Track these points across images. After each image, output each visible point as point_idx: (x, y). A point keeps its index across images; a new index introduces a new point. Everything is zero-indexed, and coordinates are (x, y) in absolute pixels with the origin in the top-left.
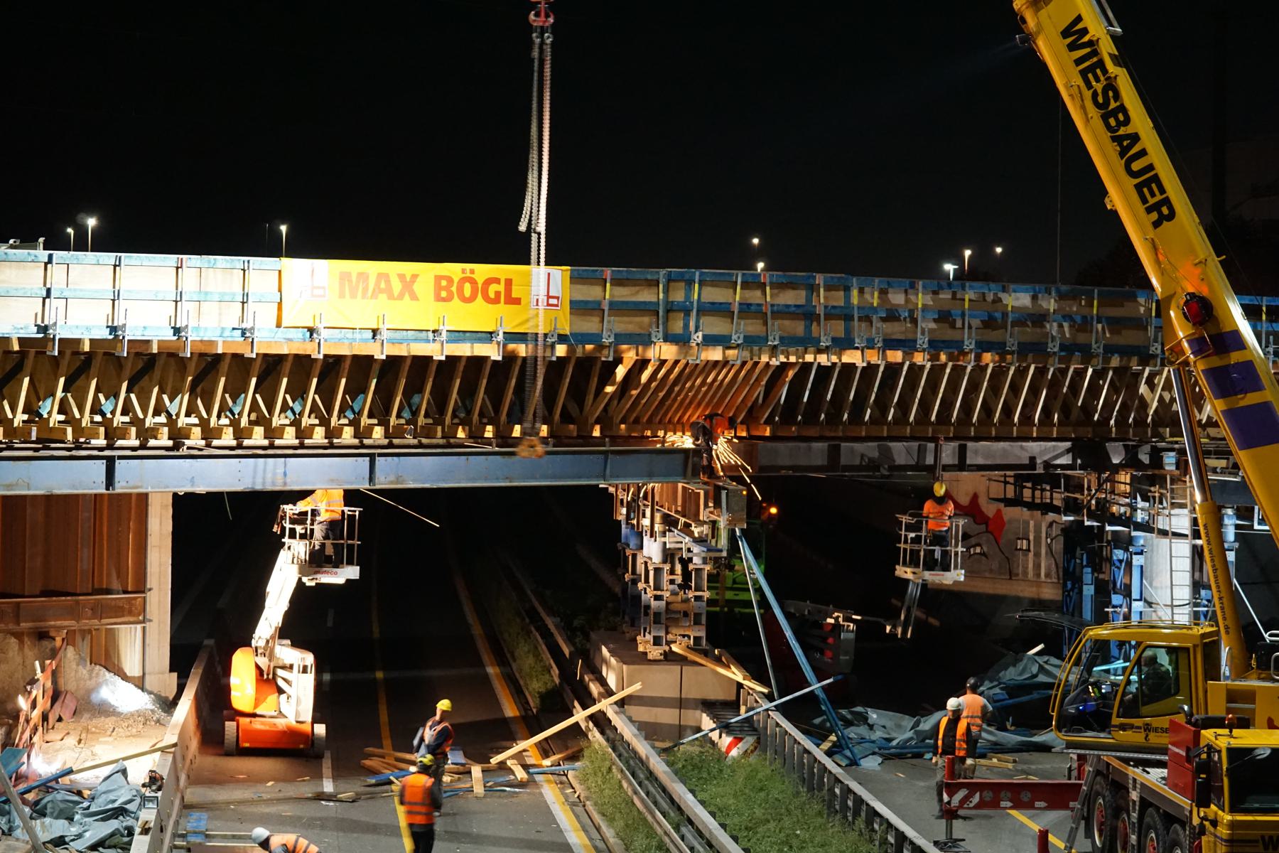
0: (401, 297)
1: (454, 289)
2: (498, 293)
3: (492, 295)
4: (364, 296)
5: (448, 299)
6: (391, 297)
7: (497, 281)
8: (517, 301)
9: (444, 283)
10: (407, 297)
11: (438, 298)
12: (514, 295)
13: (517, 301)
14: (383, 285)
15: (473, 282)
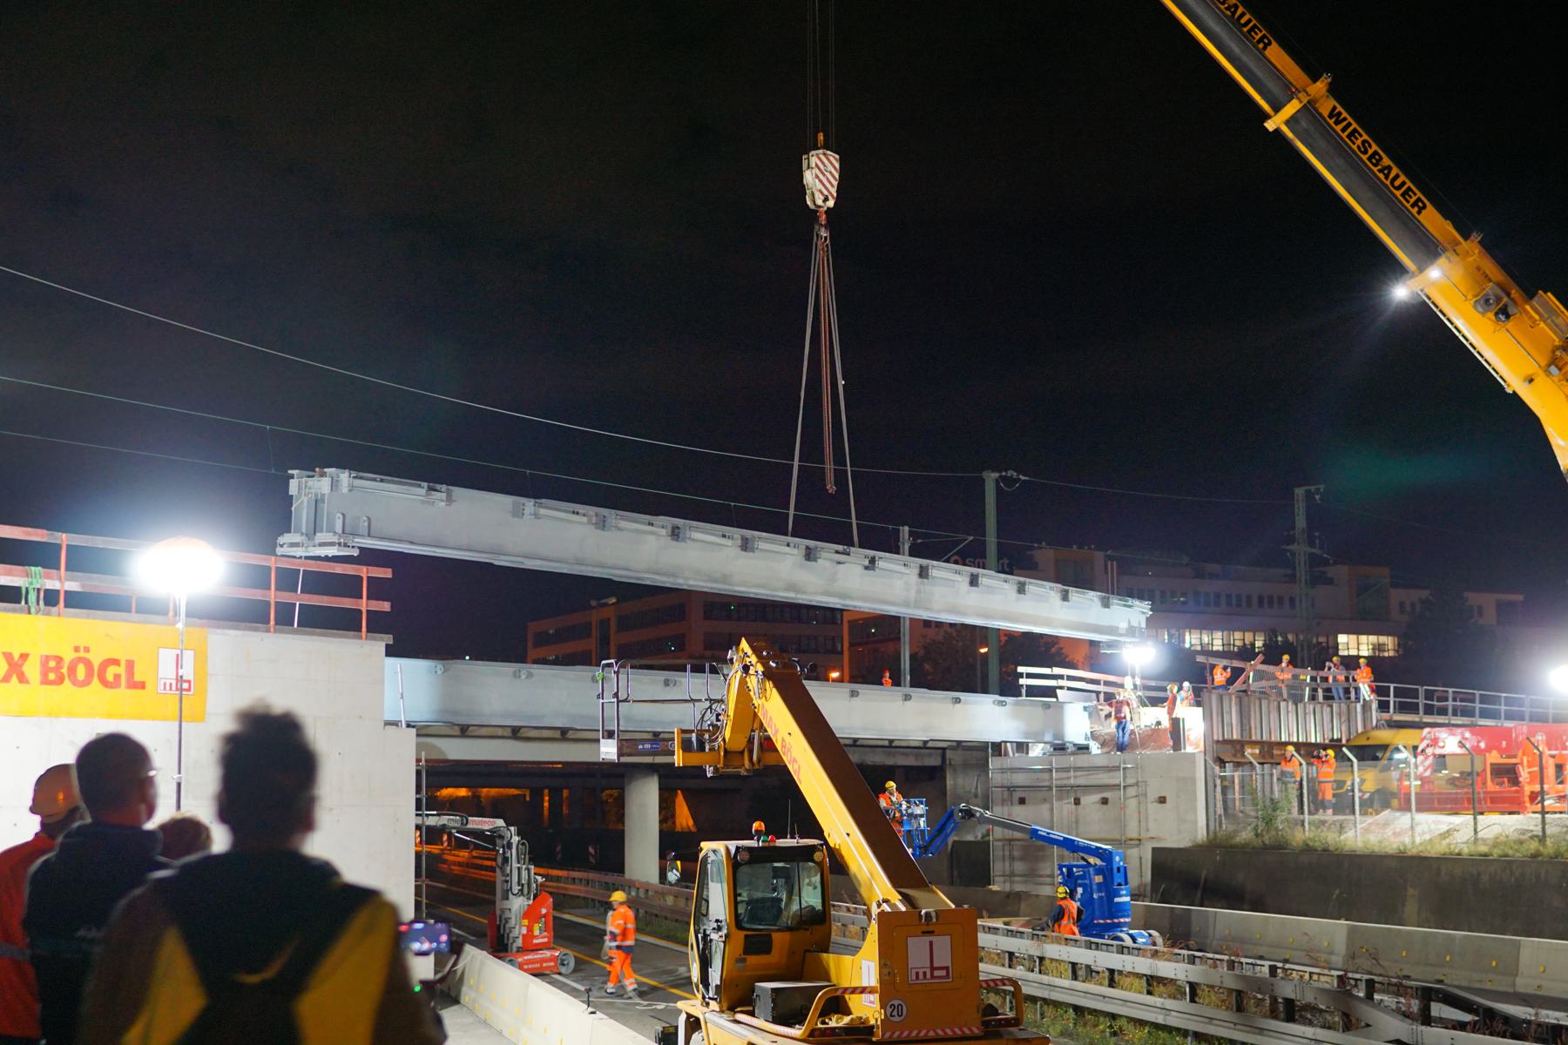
1: (64, 671)
2: (117, 677)
3: (110, 678)
5: (60, 680)
7: (116, 662)
8: (142, 686)
9: (52, 664)
10: (14, 678)
11: (45, 681)
12: (138, 677)
13: (142, 686)
15: (88, 664)
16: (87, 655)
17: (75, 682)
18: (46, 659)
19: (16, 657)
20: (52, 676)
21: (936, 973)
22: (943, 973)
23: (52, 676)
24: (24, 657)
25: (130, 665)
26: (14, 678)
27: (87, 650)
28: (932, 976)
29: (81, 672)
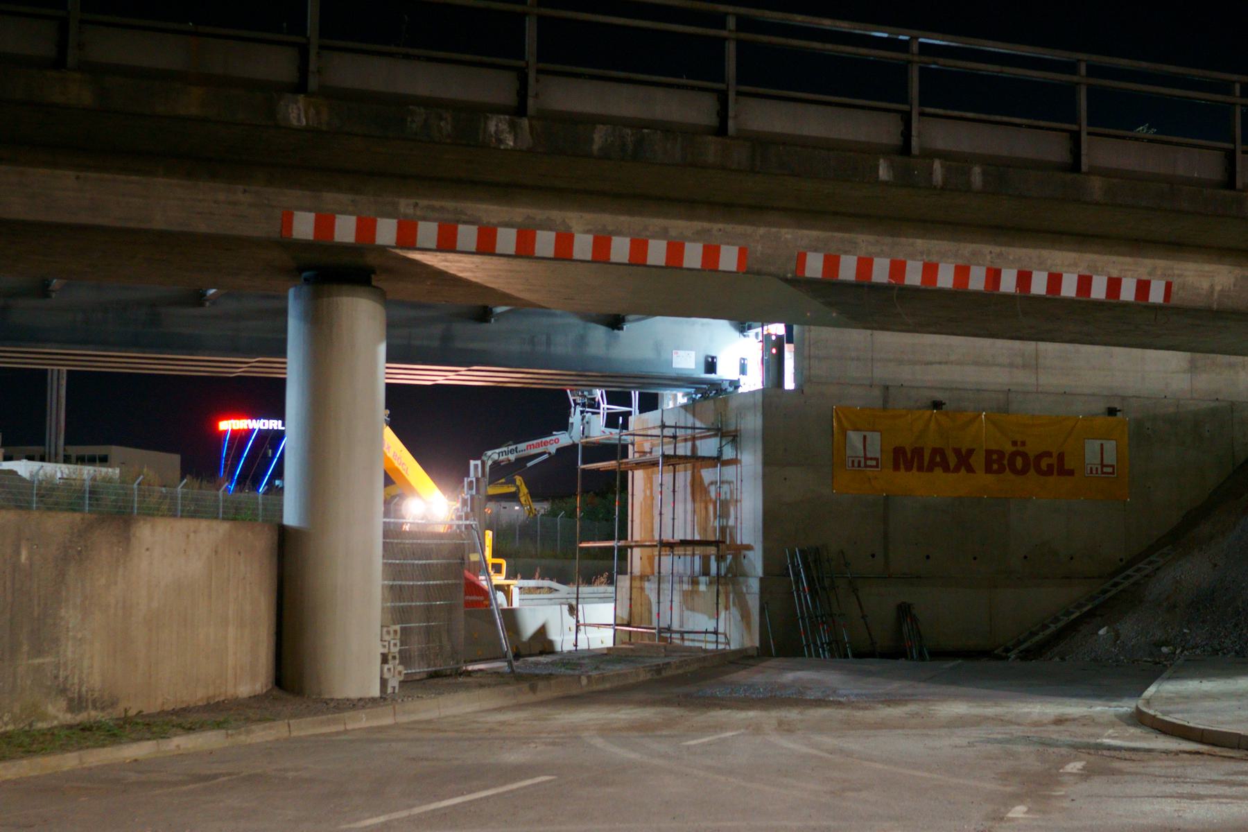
0: (957, 469)
1: (1006, 462)
2: (1050, 466)
4: (920, 469)
5: (1001, 470)
6: (946, 469)
8: (1071, 473)
10: (963, 471)
11: (988, 470)
13: (1071, 473)
14: (938, 459)
15: (1024, 455)
16: (1021, 449)
17: (1014, 470)
18: (989, 453)
19: (964, 451)
20: (995, 466)
21: (1105, 470)
22: (1110, 470)
23: (995, 466)
24: (970, 452)
25: (1061, 457)
26: (963, 471)
27: (1023, 444)
28: (1103, 473)
29: (1019, 462)
